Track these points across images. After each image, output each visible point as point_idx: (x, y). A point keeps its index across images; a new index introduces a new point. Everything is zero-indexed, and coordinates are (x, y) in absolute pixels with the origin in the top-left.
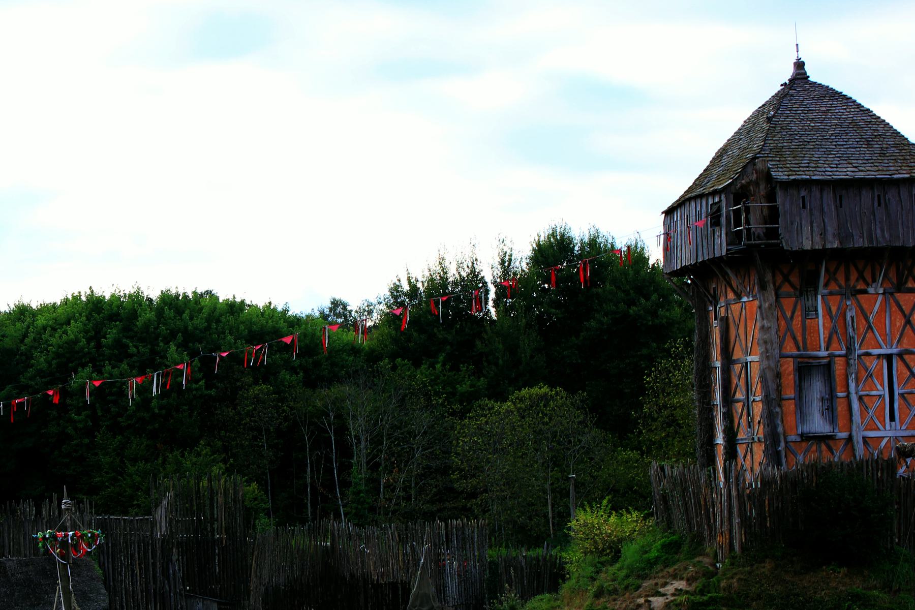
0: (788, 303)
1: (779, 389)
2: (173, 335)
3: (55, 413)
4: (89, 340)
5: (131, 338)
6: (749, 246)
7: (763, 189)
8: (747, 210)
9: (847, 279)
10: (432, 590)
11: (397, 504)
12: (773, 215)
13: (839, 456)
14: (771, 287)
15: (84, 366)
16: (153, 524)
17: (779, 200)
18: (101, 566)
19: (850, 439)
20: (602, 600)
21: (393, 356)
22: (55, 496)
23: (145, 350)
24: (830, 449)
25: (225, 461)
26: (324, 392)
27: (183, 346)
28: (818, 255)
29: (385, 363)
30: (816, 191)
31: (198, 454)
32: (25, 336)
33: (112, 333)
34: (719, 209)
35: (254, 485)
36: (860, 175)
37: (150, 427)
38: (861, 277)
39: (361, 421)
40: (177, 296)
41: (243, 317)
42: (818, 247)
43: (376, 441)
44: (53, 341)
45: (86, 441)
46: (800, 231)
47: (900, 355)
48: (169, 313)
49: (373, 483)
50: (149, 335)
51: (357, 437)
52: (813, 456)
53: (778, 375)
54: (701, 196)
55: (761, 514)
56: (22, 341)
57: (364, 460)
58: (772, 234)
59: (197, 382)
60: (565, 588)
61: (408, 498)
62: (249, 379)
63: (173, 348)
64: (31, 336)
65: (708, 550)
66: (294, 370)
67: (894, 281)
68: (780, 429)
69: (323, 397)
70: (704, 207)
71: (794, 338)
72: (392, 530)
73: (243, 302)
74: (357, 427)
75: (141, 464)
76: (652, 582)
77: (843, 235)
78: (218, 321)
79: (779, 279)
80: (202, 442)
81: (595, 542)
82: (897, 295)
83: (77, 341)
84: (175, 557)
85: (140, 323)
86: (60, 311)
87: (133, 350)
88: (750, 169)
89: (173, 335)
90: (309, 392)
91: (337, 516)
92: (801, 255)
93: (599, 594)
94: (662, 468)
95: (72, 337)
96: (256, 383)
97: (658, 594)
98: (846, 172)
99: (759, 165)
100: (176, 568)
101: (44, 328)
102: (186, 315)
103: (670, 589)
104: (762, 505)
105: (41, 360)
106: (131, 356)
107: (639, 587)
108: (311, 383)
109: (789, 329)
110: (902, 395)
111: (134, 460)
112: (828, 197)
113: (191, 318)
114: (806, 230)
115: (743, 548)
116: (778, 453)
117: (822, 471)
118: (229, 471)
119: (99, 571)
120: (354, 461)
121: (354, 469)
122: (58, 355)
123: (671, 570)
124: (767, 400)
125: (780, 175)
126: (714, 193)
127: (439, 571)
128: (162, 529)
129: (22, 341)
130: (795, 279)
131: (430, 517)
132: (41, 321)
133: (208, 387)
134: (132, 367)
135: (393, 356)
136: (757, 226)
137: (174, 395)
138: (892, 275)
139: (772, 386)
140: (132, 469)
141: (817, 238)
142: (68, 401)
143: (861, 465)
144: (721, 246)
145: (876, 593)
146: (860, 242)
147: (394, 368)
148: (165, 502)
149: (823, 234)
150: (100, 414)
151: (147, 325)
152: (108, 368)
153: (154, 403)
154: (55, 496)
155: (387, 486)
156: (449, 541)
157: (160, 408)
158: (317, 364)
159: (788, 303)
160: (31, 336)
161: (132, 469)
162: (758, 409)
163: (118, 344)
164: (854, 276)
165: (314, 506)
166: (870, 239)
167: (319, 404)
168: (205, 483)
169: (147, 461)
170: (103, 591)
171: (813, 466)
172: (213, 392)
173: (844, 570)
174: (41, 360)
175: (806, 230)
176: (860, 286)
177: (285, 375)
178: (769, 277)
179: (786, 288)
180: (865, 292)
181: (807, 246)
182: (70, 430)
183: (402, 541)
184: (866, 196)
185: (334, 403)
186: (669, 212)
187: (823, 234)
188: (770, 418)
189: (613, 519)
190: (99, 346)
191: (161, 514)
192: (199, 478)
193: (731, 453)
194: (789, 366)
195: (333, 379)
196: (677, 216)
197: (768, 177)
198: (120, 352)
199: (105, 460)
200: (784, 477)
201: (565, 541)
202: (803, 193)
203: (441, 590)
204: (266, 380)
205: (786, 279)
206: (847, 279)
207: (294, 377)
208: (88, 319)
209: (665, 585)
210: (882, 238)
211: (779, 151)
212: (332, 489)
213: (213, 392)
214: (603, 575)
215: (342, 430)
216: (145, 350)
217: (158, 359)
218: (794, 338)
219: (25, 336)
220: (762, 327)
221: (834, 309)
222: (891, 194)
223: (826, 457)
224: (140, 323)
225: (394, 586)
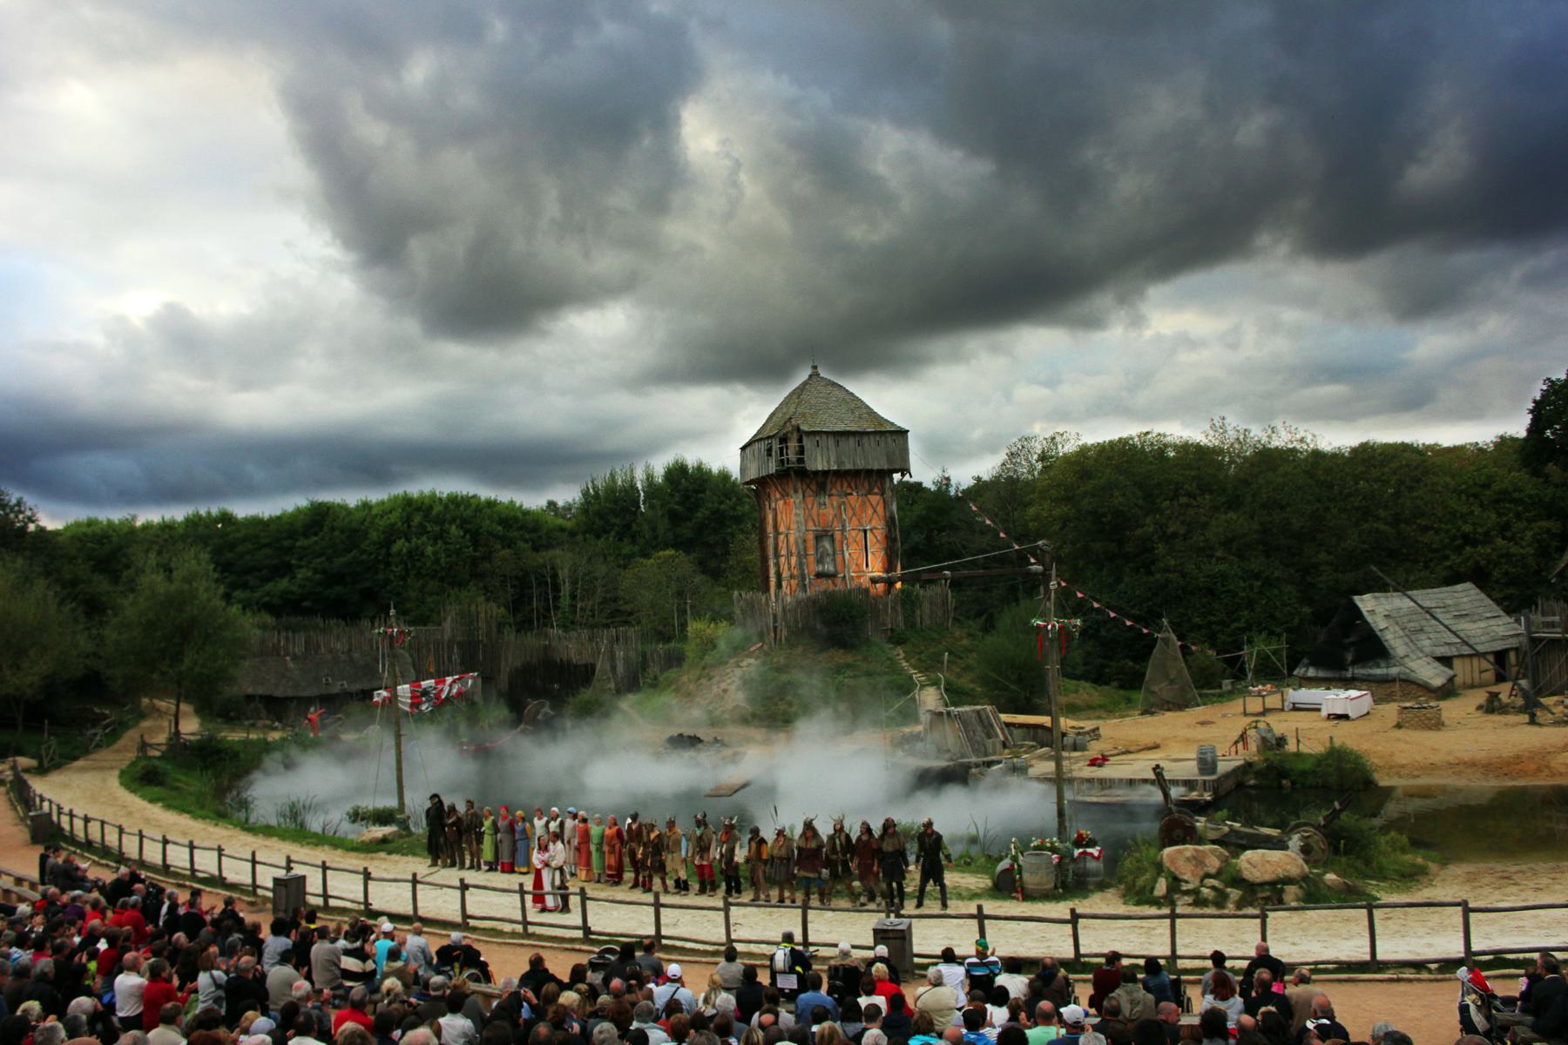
0: (809, 500)
1: (805, 549)
2: (454, 520)
3: (382, 567)
4: (403, 523)
5: (429, 522)
6: (789, 468)
7: (795, 435)
8: (787, 448)
9: (842, 487)
10: (608, 667)
11: (587, 619)
12: (801, 451)
13: (840, 586)
14: (800, 491)
15: (400, 538)
16: (443, 631)
17: (805, 442)
18: (411, 656)
19: (844, 577)
20: (707, 671)
21: (585, 533)
22: (383, 616)
23: (437, 528)
24: (834, 583)
25: (485, 595)
26: (544, 553)
27: (460, 527)
28: (825, 473)
29: (580, 537)
30: (824, 437)
31: (469, 591)
32: (365, 520)
33: (417, 519)
34: (771, 447)
35: (502, 609)
36: (848, 429)
37: (439, 575)
38: (849, 486)
39: (566, 570)
40: (457, 496)
41: (496, 509)
42: (826, 469)
43: (574, 583)
44: (381, 523)
45: (401, 583)
46: (816, 460)
47: (871, 530)
48: (452, 507)
49: (574, 607)
50: (440, 520)
51: (564, 582)
52: (825, 587)
53: (805, 541)
54: (761, 439)
55: (797, 622)
56: (362, 523)
57: (567, 594)
58: (801, 461)
59: (468, 548)
60: (685, 667)
61: (593, 616)
62: (499, 547)
63: (454, 527)
64: (368, 520)
65: (767, 641)
66: (526, 541)
67: (867, 487)
68: (806, 571)
69: (543, 557)
70: (763, 446)
71: (813, 520)
72: (585, 633)
73: (496, 501)
74: (564, 574)
75: (435, 597)
76: (735, 660)
77: (839, 463)
78: (480, 511)
79: (805, 487)
80: (471, 584)
81: (702, 639)
82: (869, 496)
83: (395, 523)
84: (455, 651)
85: (434, 512)
86: (386, 505)
87: (429, 529)
88: (788, 424)
89: (454, 520)
90: (535, 554)
91: (552, 627)
92: (816, 473)
93: (704, 668)
94: (741, 595)
95: (393, 521)
96: (503, 548)
97: (739, 666)
98: (840, 427)
99: (793, 422)
100: (455, 657)
101: (376, 515)
102: (462, 508)
103: (744, 663)
104: (796, 613)
105: (374, 535)
106: (428, 532)
107: (727, 663)
108: (536, 549)
109: (810, 515)
110: (872, 553)
111: (431, 594)
112: (831, 441)
113: (465, 510)
114: (819, 459)
115: (787, 639)
116: (805, 585)
117: (830, 596)
118: (488, 600)
119: (409, 660)
120: (562, 594)
121: (562, 600)
122: (384, 532)
123: (746, 652)
124: (799, 556)
125: (805, 428)
126: (768, 438)
127: (613, 658)
128: (448, 634)
129: (362, 523)
130: (814, 487)
131: (607, 626)
132: (374, 511)
133: (475, 551)
134: (429, 539)
135: (585, 533)
136: (792, 456)
137: (454, 556)
138: (866, 484)
139: (801, 547)
140: (429, 600)
141: (825, 464)
142: (390, 559)
143: (850, 592)
144: (772, 468)
145: (859, 663)
146: (848, 466)
147: (585, 540)
148: (449, 618)
149: (828, 462)
150: (409, 566)
151: (438, 514)
152: (415, 539)
153: (442, 560)
154: (383, 616)
155: (581, 609)
156: (618, 639)
157: (447, 563)
158: (540, 537)
159: (809, 500)
160: (368, 520)
161: (429, 600)
162: (794, 560)
163: (421, 525)
164: (845, 485)
165: (538, 620)
166: (854, 465)
167: (541, 561)
168: (473, 608)
169: (438, 594)
170: (412, 671)
171: (825, 592)
172: (477, 554)
173: (842, 651)
174: (374, 535)
175: (819, 459)
176: (849, 491)
177: (521, 544)
178: (799, 485)
179: (808, 492)
180: (851, 494)
181: (820, 468)
182: (392, 577)
183: (591, 640)
184: (852, 440)
185: (550, 560)
186: (743, 449)
187: (828, 462)
188: (801, 565)
189: (712, 625)
190: (409, 526)
191: (447, 625)
192: (469, 605)
193: (779, 586)
194: (811, 536)
195: (548, 547)
196: (747, 450)
197: (798, 429)
198: (422, 531)
199: (413, 594)
200: (809, 599)
201: (684, 638)
202: (818, 438)
203: (614, 668)
204: (509, 547)
205: (808, 486)
206: (842, 487)
207: (526, 546)
208: (403, 510)
209: (742, 661)
210: (861, 465)
211: (804, 415)
212: (548, 610)
213: (477, 554)
214: (707, 657)
215: (555, 576)
216: (437, 528)
217: (445, 535)
218: (813, 520)
219: (365, 520)
220: (796, 514)
221: (835, 504)
222: (865, 440)
223: (831, 588)
224: (434, 512)
225: (586, 666)
